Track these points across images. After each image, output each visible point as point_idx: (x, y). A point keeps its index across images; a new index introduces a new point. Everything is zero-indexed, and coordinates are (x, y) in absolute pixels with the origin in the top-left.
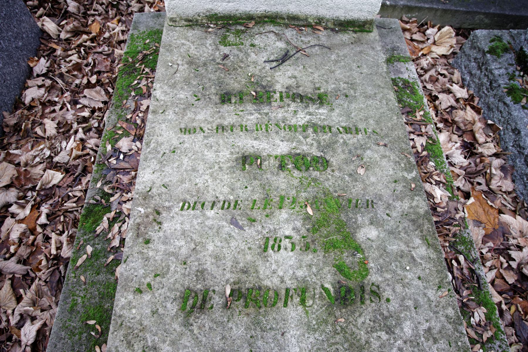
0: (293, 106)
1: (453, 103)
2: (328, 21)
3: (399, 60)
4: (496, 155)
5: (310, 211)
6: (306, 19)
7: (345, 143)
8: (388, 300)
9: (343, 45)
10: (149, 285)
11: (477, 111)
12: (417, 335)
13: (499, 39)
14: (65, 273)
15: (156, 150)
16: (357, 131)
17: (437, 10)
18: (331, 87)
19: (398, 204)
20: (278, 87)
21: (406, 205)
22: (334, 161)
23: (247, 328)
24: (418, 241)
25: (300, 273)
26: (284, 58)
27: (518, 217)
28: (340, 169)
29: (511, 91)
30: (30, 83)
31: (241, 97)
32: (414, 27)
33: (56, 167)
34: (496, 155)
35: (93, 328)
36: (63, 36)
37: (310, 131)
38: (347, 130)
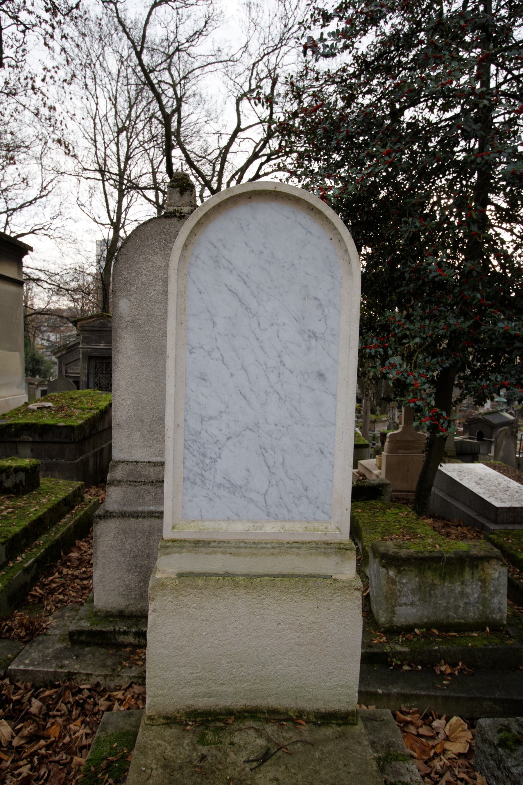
2: (309, 713)
3: (396, 759)
6: (287, 713)
9: (327, 740)
13: (508, 729)
17: (436, 697)
32: (416, 718)
36: (16, 742)
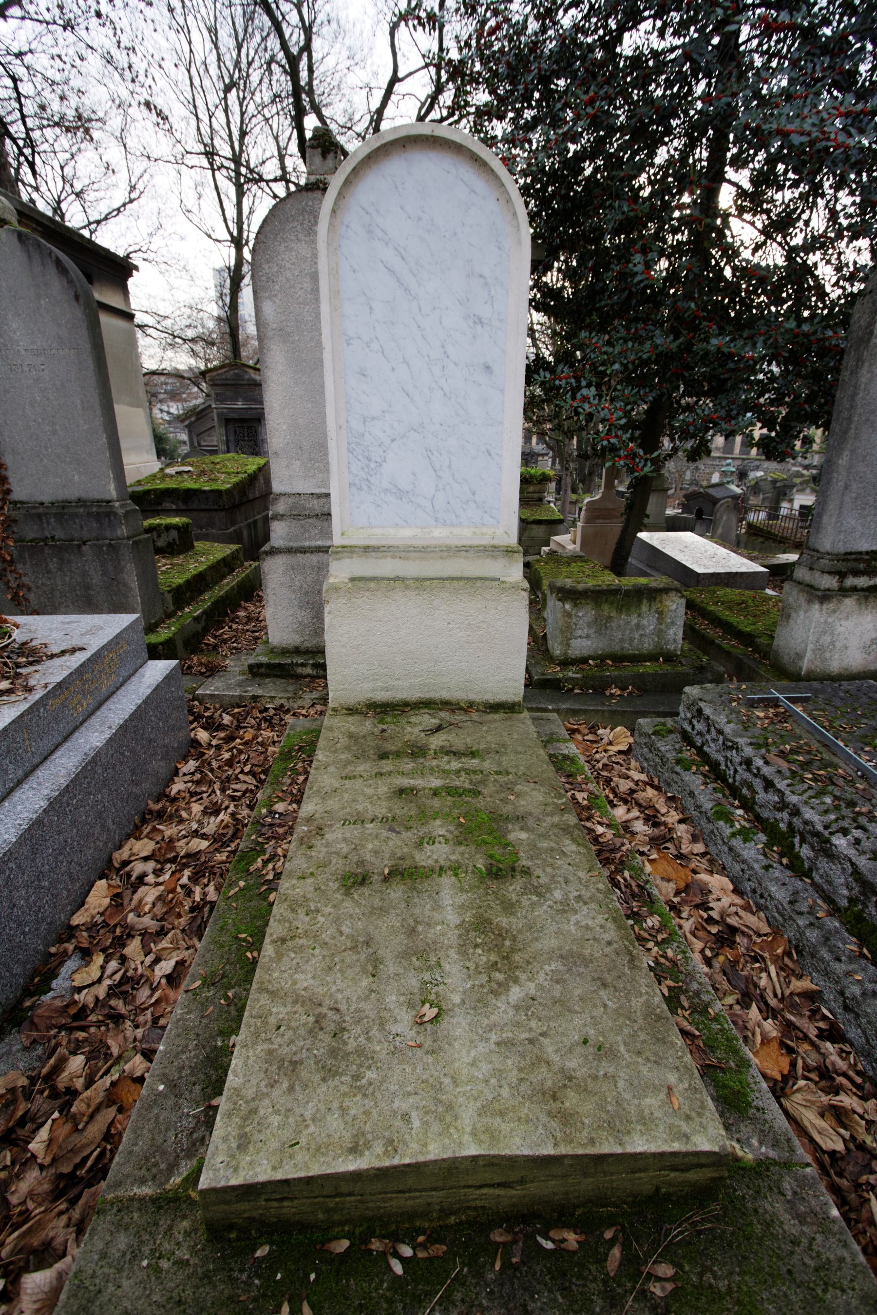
0: (446, 758)
1: (632, 785)
2: (478, 704)
3: (558, 741)
4: (681, 821)
5: (462, 820)
6: (458, 704)
7: (495, 780)
8: (538, 877)
9: (495, 721)
10: (312, 874)
11: (657, 788)
12: (568, 899)
13: (664, 724)
14: (95, 1150)
15: (318, 791)
16: (508, 773)
17: (603, 711)
18: (482, 746)
19: (548, 819)
20: (433, 747)
21: (556, 819)
22: (485, 792)
23: (404, 892)
24: (568, 842)
25: (453, 857)
26: (439, 728)
27: (716, 876)
28: (491, 796)
29: (678, 762)
30: (176, 779)
31: (398, 754)
32: (584, 729)
33: (204, 836)
34: (681, 821)
35: (245, 940)
36: (214, 742)
37: (463, 773)
38: (498, 773)
